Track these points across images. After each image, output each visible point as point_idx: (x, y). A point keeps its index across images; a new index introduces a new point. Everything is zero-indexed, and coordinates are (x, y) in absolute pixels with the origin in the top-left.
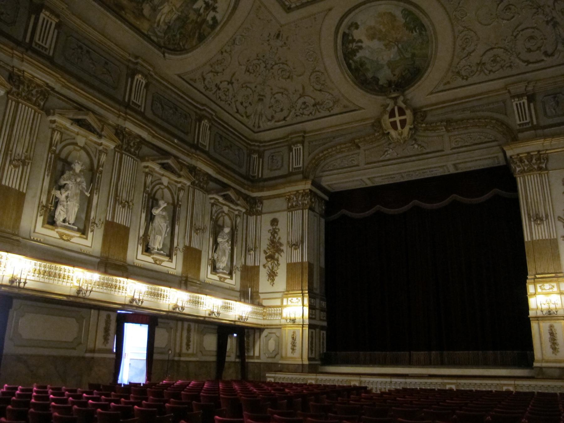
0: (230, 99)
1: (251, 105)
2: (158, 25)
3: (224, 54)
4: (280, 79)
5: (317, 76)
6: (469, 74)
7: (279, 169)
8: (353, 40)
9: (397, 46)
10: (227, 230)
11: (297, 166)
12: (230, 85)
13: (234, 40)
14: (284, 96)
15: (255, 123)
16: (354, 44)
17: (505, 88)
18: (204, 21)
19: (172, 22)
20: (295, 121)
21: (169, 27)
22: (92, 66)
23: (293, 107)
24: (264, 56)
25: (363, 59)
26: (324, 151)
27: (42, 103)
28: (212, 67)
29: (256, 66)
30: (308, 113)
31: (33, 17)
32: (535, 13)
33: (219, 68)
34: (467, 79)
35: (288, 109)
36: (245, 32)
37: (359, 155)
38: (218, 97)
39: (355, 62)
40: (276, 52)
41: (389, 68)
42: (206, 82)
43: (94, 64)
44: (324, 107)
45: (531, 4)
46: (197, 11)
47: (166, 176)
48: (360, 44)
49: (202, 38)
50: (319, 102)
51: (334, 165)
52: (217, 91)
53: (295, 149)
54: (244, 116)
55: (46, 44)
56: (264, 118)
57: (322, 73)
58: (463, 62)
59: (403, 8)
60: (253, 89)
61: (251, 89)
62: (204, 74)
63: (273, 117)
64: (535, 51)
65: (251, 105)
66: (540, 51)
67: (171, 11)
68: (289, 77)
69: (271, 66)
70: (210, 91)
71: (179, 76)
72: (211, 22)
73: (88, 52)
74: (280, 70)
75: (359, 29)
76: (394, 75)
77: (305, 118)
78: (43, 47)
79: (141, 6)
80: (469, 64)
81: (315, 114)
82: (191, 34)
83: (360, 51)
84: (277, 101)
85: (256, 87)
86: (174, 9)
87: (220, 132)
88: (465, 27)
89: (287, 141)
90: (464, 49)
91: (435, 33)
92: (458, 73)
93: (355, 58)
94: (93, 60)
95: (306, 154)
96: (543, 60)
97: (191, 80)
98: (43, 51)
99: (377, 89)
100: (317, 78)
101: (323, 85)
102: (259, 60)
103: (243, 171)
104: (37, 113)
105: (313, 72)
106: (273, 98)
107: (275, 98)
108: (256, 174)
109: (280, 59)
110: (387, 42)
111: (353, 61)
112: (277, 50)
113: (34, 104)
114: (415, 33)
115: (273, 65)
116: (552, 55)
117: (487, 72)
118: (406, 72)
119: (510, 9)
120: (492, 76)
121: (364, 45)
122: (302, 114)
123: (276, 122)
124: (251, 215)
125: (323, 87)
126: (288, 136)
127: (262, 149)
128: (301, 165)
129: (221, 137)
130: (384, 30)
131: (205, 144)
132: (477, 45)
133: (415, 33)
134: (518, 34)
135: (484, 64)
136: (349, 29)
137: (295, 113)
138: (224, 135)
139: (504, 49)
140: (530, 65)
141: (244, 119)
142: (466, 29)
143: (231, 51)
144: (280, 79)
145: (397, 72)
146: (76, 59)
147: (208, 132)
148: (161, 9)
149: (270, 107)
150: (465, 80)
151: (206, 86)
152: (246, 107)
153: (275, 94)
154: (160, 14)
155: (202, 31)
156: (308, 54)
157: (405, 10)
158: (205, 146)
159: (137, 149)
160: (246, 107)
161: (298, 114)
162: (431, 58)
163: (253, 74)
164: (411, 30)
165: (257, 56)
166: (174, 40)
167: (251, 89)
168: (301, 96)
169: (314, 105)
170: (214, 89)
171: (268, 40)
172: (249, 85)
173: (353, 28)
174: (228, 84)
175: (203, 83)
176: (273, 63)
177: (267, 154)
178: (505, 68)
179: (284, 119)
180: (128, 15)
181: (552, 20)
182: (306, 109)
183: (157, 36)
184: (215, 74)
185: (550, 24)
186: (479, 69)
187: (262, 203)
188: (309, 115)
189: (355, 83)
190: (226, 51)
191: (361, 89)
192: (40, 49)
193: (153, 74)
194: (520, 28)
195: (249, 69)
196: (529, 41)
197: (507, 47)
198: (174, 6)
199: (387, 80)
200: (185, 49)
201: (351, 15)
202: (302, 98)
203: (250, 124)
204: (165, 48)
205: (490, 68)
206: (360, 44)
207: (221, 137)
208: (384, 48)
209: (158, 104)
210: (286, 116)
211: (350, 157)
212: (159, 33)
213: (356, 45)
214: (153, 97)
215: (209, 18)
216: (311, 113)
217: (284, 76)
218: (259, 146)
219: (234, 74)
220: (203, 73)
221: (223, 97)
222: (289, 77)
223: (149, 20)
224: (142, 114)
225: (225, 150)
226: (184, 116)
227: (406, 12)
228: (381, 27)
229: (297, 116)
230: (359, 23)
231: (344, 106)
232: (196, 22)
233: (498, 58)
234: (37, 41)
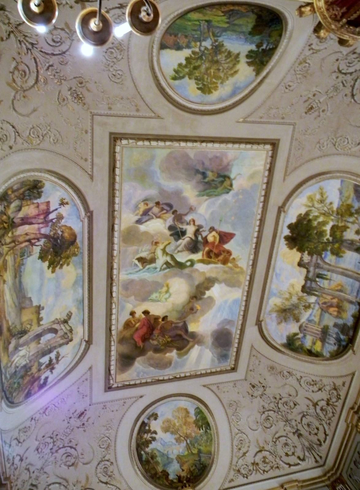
3: (33, 421)
6: (248, 473)
8: (149, 431)
9: (186, 441)
13: (46, 409)
16: (149, 435)
17: (282, 486)
24: (57, 435)
25: (155, 452)
29: (46, 445)
32: (285, 425)
33: (22, 437)
34: (247, 478)
36: (59, 402)
39: (147, 453)
40: (69, 433)
41: (178, 462)
45: (281, 417)
46: (40, 365)
48: (154, 435)
57: (112, 463)
58: (241, 462)
59: (197, 406)
64: (291, 456)
66: (295, 455)
67: (24, 356)
69: (57, 449)
72: (42, 382)
74: (66, 455)
75: (158, 420)
76: (183, 470)
80: (246, 463)
83: (153, 442)
86: (27, 356)
88: (239, 430)
90: (240, 449)
91: (217, 433)
92: (239, 471)
93: (147, 450)
96: (298, 464)
99: (167, 484)
100: (105, 468)
101: (110, 476)
105: (102, 461)
109: (71, 441)
110: (178, 436)
111: (145, 452)
112: (72, 431)
114: (202, 431)
115: (60, 448)
116: (303, 460)
117: (262, 472)
118: (194, 467)
119: (269, 419)
120: (266, 476)
121: (157, 437)
125: (110, 479)
130: (177, 424)
132: (249, 447)
133: (202, 431)
134: (276, 441)
135: (257, 464)
136: (149, 419)
139: (270, 452)
140: (292, 467)
143: (38, 420)
144: (63, 466)
145: (185, 467)
150: (245, 479)
153: (50, 485)
156: (103, 439)
157: (198, 408)
162: (215, 454)
164: (200, 427)
173: (152, 419)
176: (61, 446)
178: (274, 468)
181: (296, 432)
185: (296, 435)
186: (255, 468)
189: (144, 477)
190: (35, 420)
191: (151, 483)
194: (277, 436)
196: (285, 446)
197: (272, 451)
199: (177, 475)
201: (154, 406)
205: (263, 468)
206: (154, 435)
208: (174, 441)
213: (151, 436)
217: (68, 463)
219: (27, 449)
220: (12, 437)
222: (73, 464)
227: (198, 411)
228: (176, 421)
230: (159, 414)
232: (33, 377)
233: (267, 460)
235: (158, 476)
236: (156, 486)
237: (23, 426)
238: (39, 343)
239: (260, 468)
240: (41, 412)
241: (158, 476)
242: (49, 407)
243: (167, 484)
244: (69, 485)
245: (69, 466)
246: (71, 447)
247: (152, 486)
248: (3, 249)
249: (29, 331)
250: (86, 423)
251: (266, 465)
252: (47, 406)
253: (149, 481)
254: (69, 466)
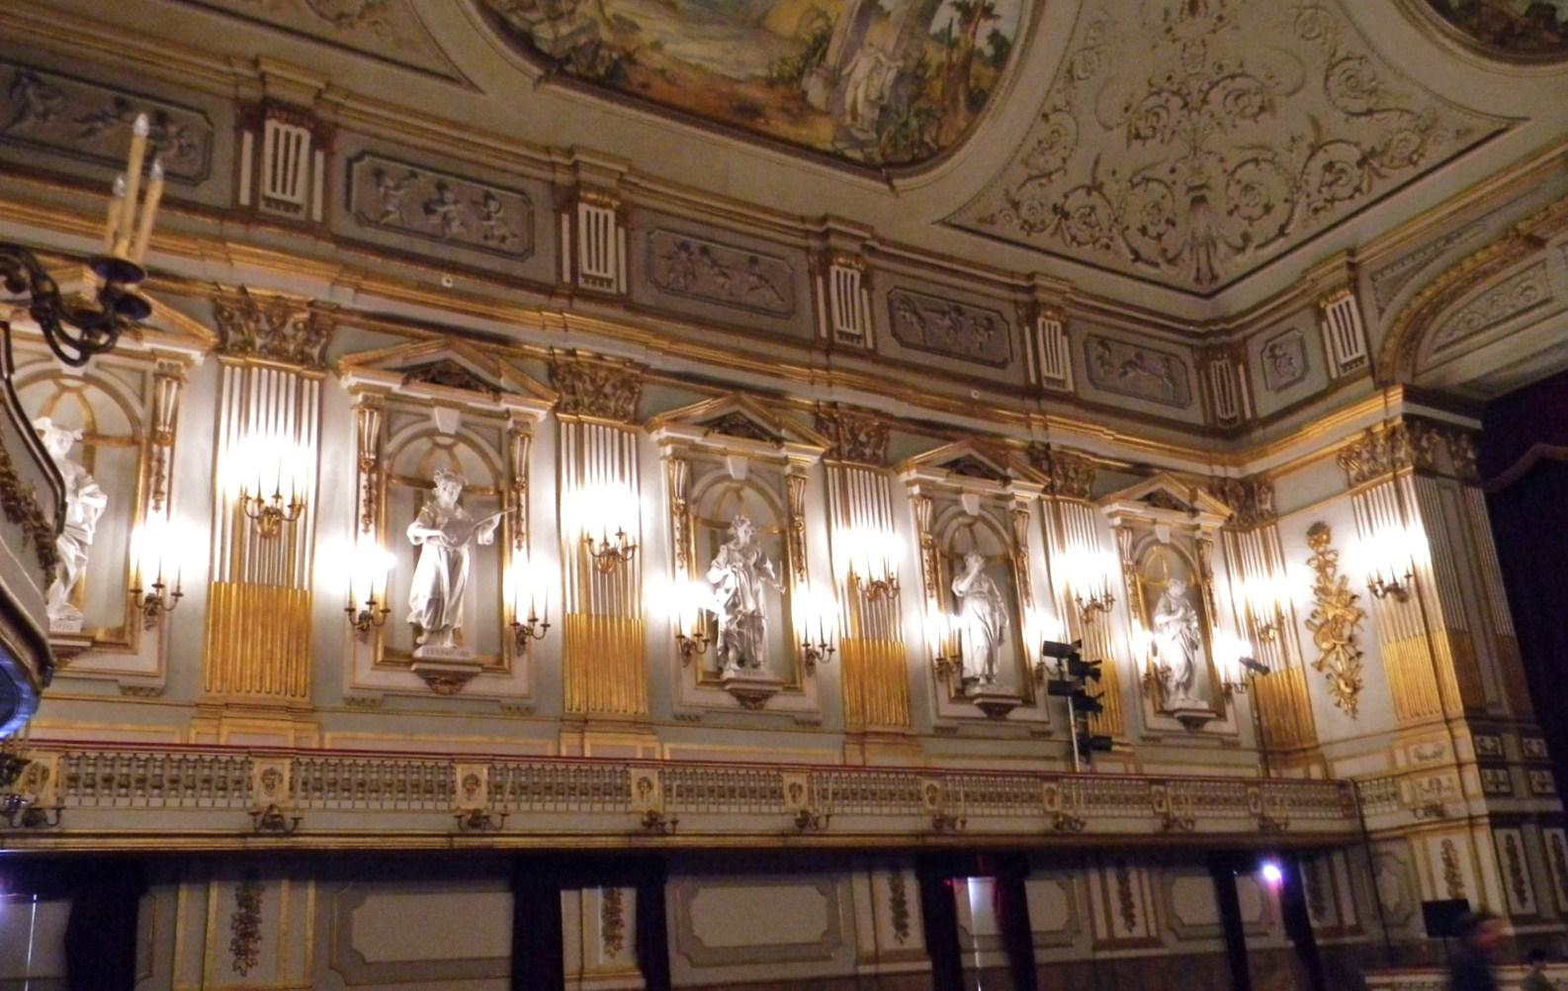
0: (1106, 231)
1: (1173, 224)
2: (854, 118)
4: (1239, 122)
5: (1349, 73)
7: (1301, 379)
10: (1176, 590)
11: (1350, 358)
12: (1095, 193)
13: (1070, 71)
14: (1263, 165)
15: (1198, 269)
18: (972, 54)
19: (887, 93)
20: (1315, 228)
21: (884, 110)
22: (721, 280)
23: (1299, 189)
24: (1169, 78)
26: (1424, 287)
27: (631, 408)
28: (1027, 165)
29: (1157, 114)
30: (1348, 191)
31: (566, 218)
37: (1544, 267)
38: (1068, 238)
42: (1024, 212)
43: (725, 275)
44: (1393, 159)
46: (945, 39)
47: (970, 492)
49: (978, 101)
50: (1373, 149)
51: (1470, 321)
52: (1059, 223)
53: (1334, 311)
54: (1160, 261)
55: (606, 271)
56: (1222, 248)
60: (1168, 178)
61: (1159, 181)
62: (1013, 190)
63: (1246, 238)
65: (1173, 224)
67: (877, 66)
68: (1262, 109)
69: (1201, 96)
70: (1042, 230)
71: (944, 223)
72: (989, 51)
73: (704, 251)
77: (1343, 208)
78: (602, 280)
79: (799, 87)
82: (947, 103)
84: (1248, 188)
85: (1173, 171)
86: (883, 59)
87: (1102, 331)
89: (1304, 292)
94: (720, 266)
95: (1371, 313)
97: (981, 220)
98: (605, 289)
99: (1555, 39)
100: (1349, 78)
101: (1372, 92)
102: (1158, 93)
103: (1195, 415)
104: (625, 435)
106: (1232, 183)
107: (1239, 182)
108: (1236, 413)
109: (1220, 67)
113: (615, 416)
115: (1207, 93)
122: (1332, 201)
124: (1247, 530)
125: (1374, 100)
126: (1302, 278)
127: (1238, 336)
128: (1362, 351)
129: (1103, 342)
131: (1061, 377)
137: (1309, 205)
138: (1111, 333)
141: (1165, 272)
143: (1068, 103)
146: (682, 280)
147: (1063, 342)
148: (849, 75)
149: (1230, 213)
151: (1026, 222)
152: (1159, 236)
153: (1234, 172)
154: (850, 88)
155: (972, 83)
158: (1063, 382)
159: (878, 445)
160: (1159, 236)
161: (1320, 204)
163: (1153, 137)
165: (1151, 85)
166: (906, 138)
167: (1159, 181)
168: (1315, 149)
169: (1361, 163)
170: (1052, 220)
171: (1169, 30)
172: (1148, 174)
174: (1089, 194)
175: (1014, 216)
176: (1206, 87)
177: (1255, 347)
179: (1282, 231)
180: (773, 122)
183: (861, 145)
184: (1044, 181)
187: (1271, 489)
188: (1351, 197)
190: (1056, 110)
191: (1500, 59)
192: (598, 288)
193: (875, 244)
195: (1137, 129)
198: (882, 50)
200: (941, 149)
202: (1321, 154)
203: (1184, 275)
204: (889, 164)
207: (1103, 342)
209: (908, 315)
210: (1283, 222)
211: (1518, 279)
212: (861, 136)
214: (890, 303)
215: (982, 42)
216: (1358, 189)
217: (1249, 111)
218: (1228, 332)
219: (1096, 163)
220: (1007, 192)
221: (1084, 234)
222: (1262, 109)
223: (828, 113)
224: (872, 356)
225: (1125, 373)
226: (985, 322)
229: (1316, 210)
231: (1458, 132)
232: (951, 67)
234: (586, 270)
235: (1518, 29)
236: (1517, 62)
237: (1032, 143)
238: (889, 14)
240: (1060, 85)
241: (1518, 29)
242: (1072, 64)
243: (1555, 39)
244: (1276, 154)
245: (1255, 116)
246: (1233, 77)
247: (1506, 67)
248: (585, 16)
249: (830, 27)
250: (1224, 12)
252: (1066, 64)
253: (1491, 57)
254: (1255, 116)
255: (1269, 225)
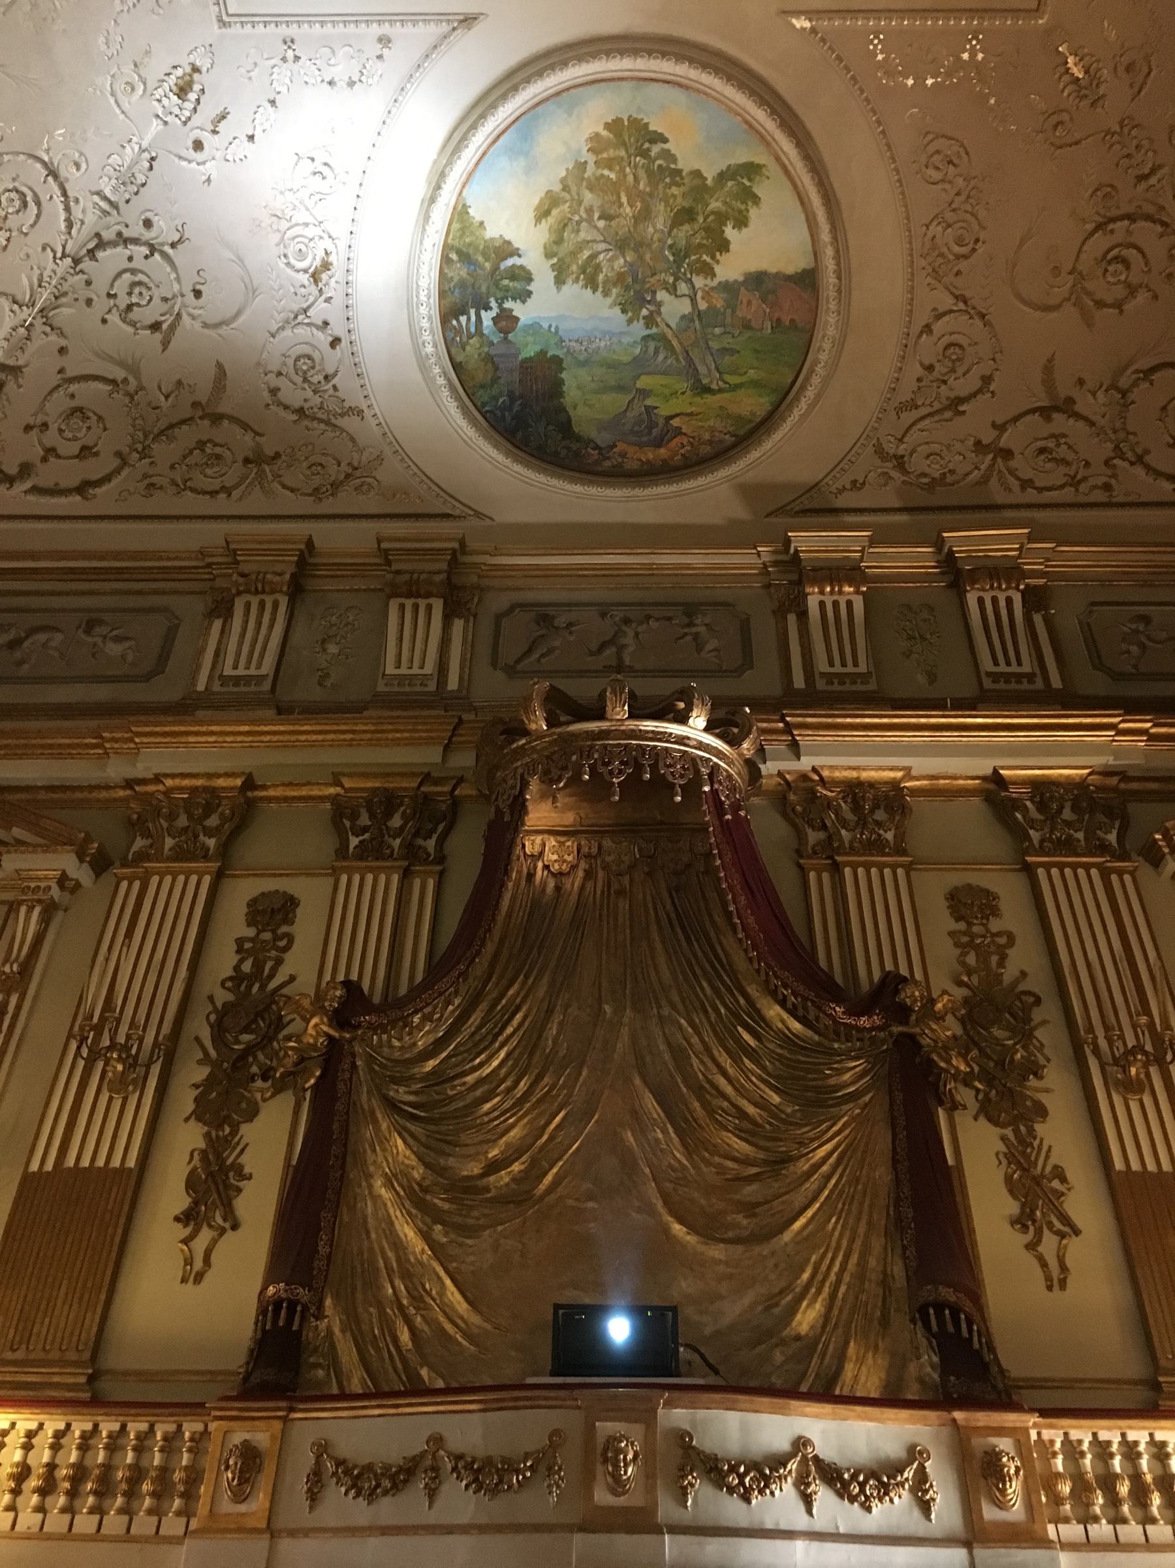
30: (216, 484)
35: (119, 454)
63: (26, 469)
81: (241, 498)
123: (36, 490)
135: (1008, 454)
142: (961, 306)
149: (28, 428)
161: (164, 481)
182: (209, 471)
239: (1012, 472)
251: (1049, 466)
255: (71, 473)
